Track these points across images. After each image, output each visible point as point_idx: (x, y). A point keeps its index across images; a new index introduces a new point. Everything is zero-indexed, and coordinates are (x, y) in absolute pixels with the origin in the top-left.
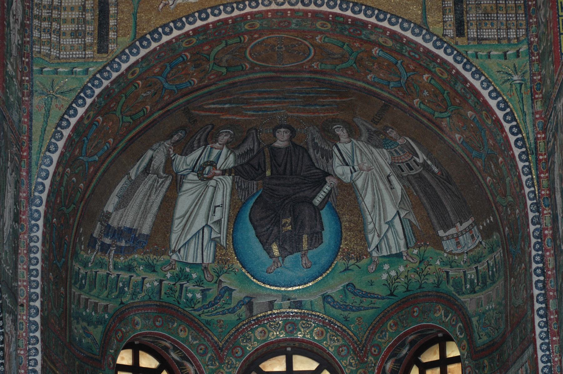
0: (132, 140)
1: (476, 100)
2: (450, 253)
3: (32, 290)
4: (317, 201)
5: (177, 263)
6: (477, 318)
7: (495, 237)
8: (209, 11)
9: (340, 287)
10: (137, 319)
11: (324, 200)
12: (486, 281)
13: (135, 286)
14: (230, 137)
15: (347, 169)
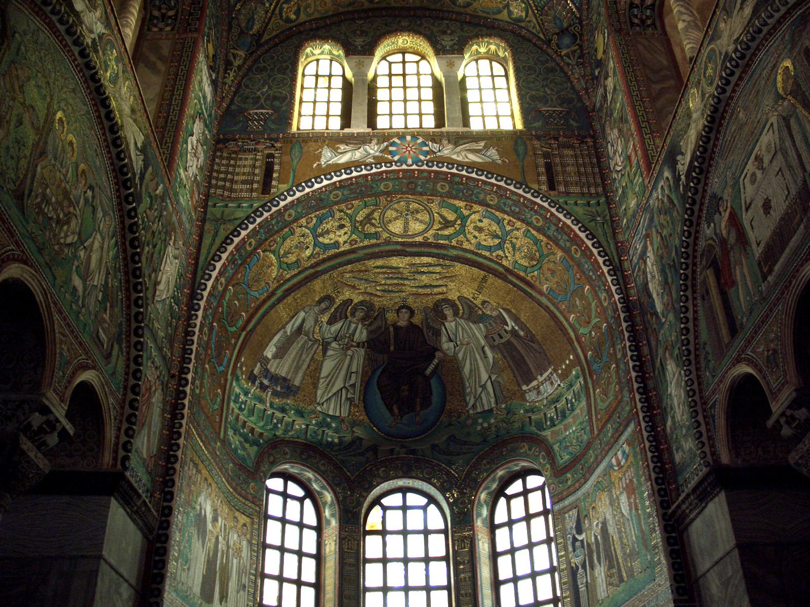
0: (288, 292)
1: (567, 238)
2: (533, 401)
3: (185, 365)
4: (428, 371)
5: (321, 414)
6: (558, 444)
7: (574, 373)
8: (353, 169)
9: (444, 438)
10: (287, 450)
11: (433, 371)
12: (565, 414)
13: (287, 425)
14: (365, 315)
15: (451, 345)
